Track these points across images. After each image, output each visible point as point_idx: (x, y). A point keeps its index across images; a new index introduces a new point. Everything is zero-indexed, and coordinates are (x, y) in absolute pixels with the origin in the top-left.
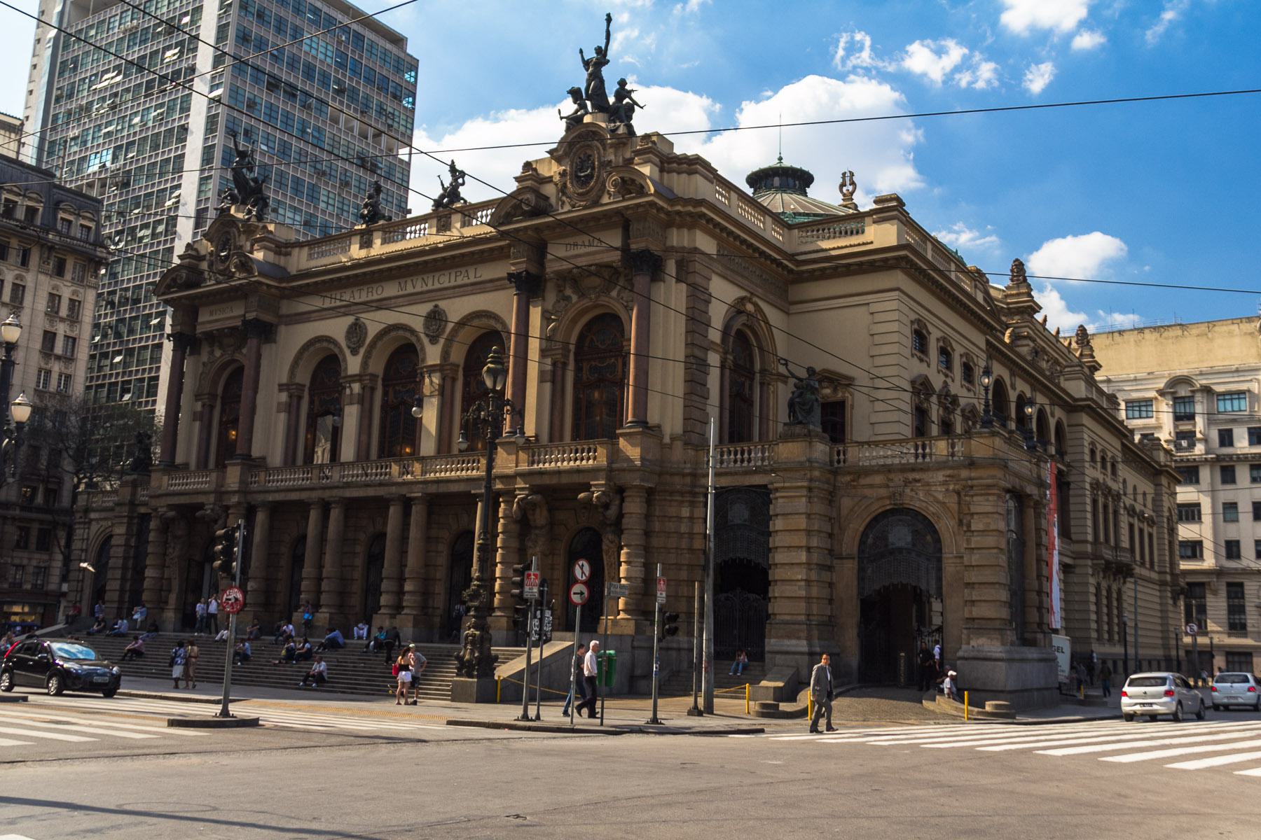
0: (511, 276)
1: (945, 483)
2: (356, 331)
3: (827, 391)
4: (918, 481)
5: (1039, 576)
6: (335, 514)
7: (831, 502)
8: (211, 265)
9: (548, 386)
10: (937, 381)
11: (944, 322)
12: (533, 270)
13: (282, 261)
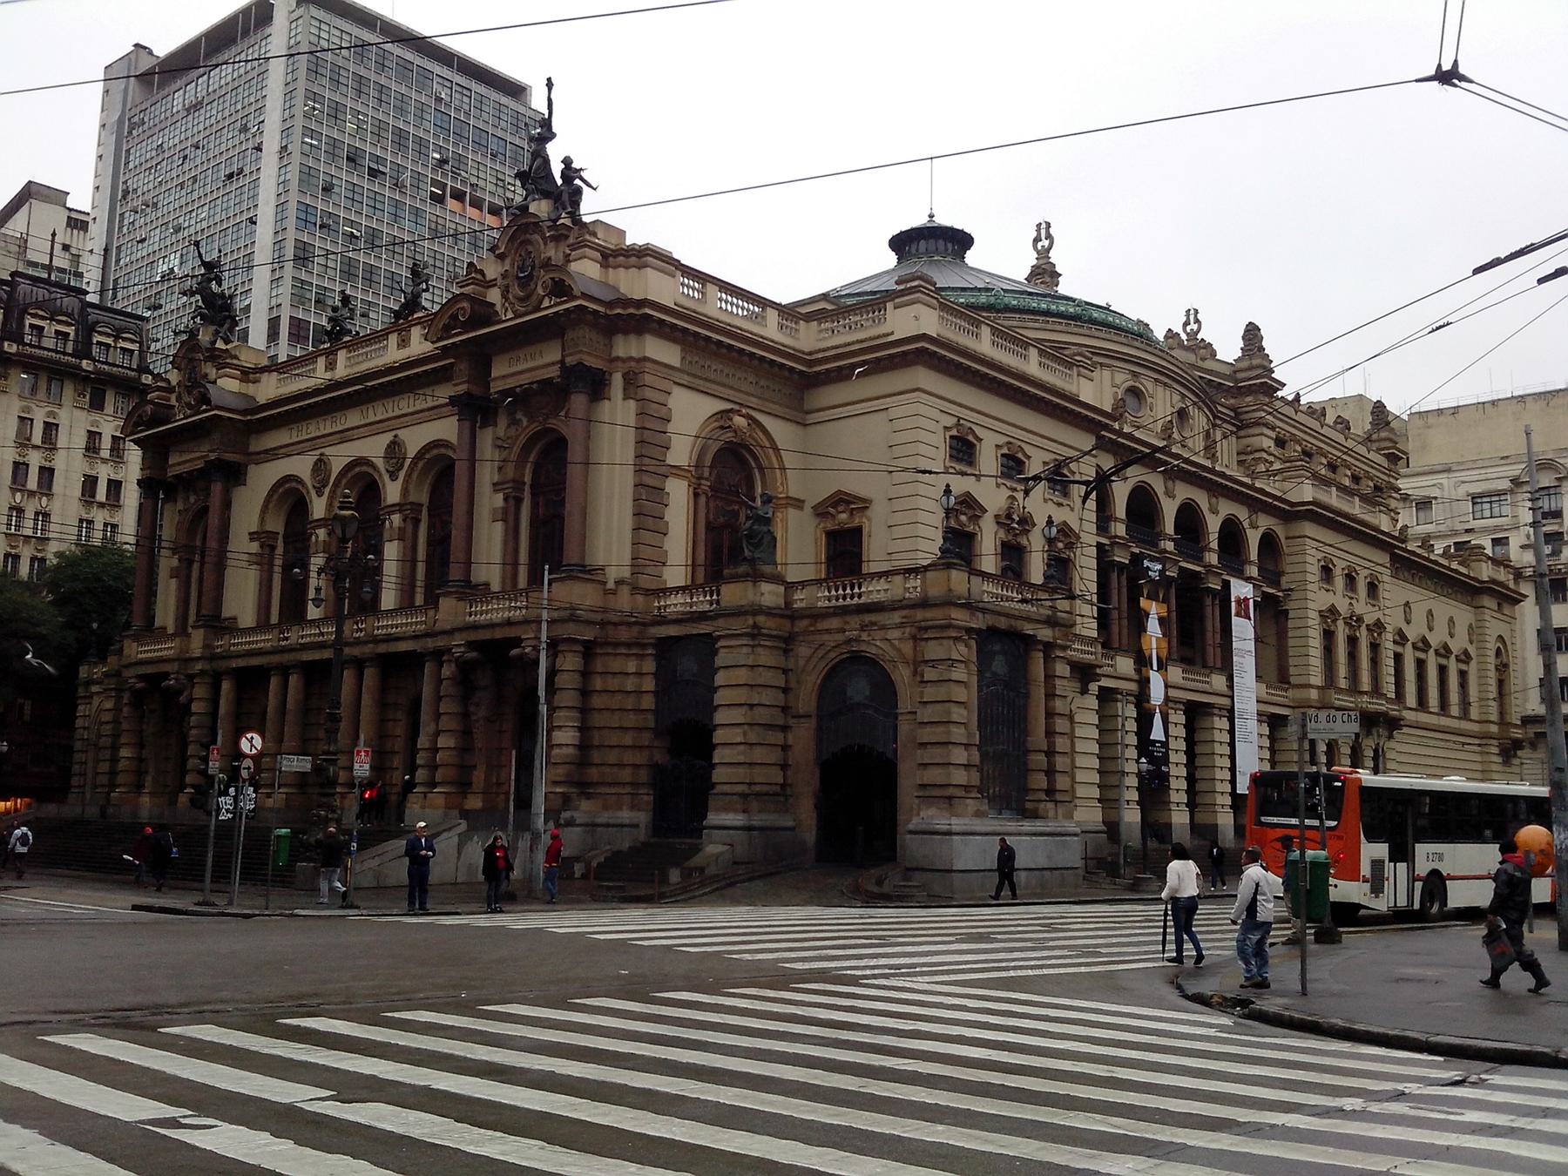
0: (453, 401)
1: (901, 626)
2: (321, 466)
3: (843, 516)
4: (874, 624)
5: (1050, 733)
6: (294, 680)
7: (786, 652)
9: (499, 526)
11: (998, 424)
12: (476, 390)
13: (250, 389)
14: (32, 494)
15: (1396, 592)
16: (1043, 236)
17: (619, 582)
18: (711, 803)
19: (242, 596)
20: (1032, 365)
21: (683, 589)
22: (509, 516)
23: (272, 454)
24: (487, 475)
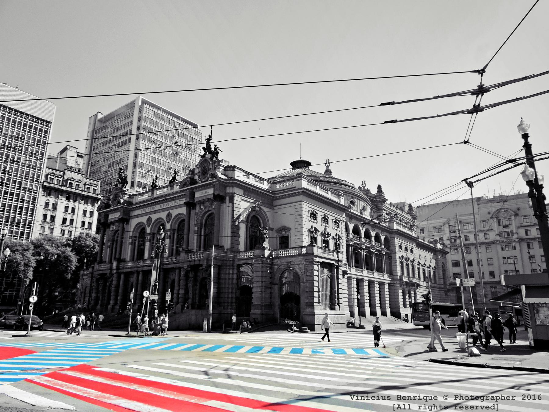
2: (149, 219)
3: (284, 233)
8: (112, 202)
10: (321, 229)
14: (68, 226)
15: (418, 251)
16: (327, 164)
17: (227, 250)
18: (252, 308)
19: (127, 254)
20: (329, 195)
21: (244, 251)
22: (199, 233)
23: (137, 216)
24: (193, 222)
